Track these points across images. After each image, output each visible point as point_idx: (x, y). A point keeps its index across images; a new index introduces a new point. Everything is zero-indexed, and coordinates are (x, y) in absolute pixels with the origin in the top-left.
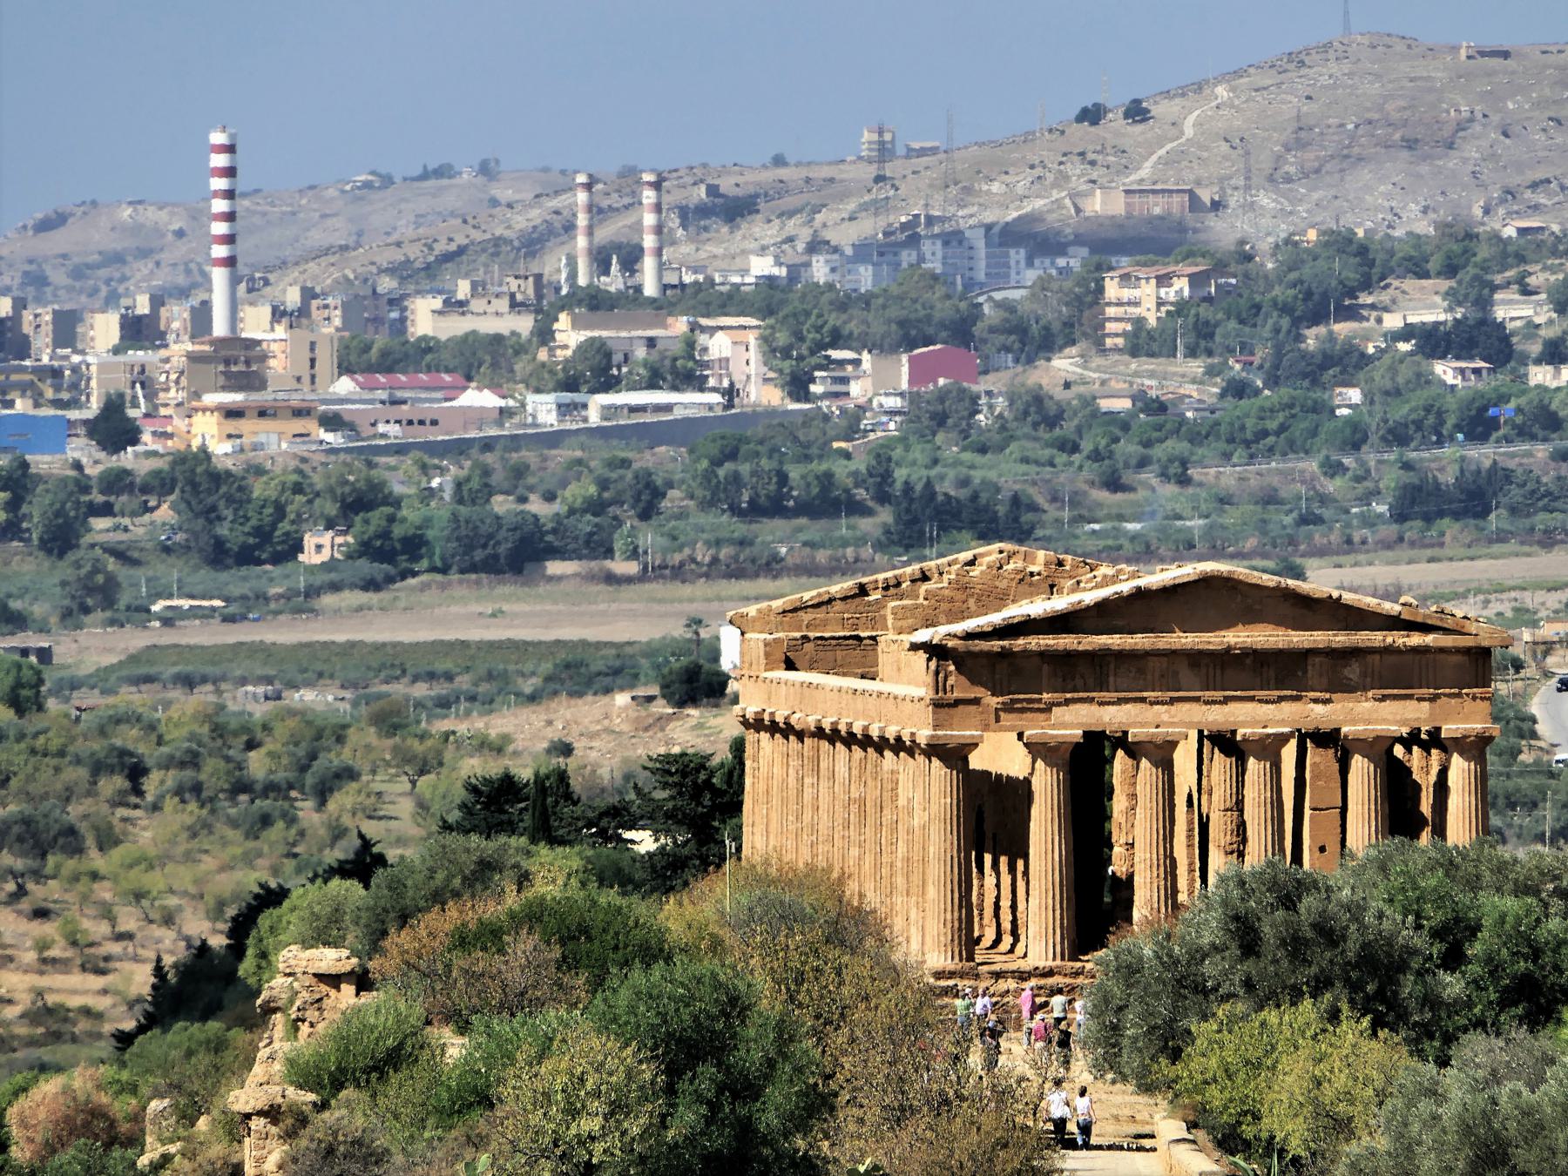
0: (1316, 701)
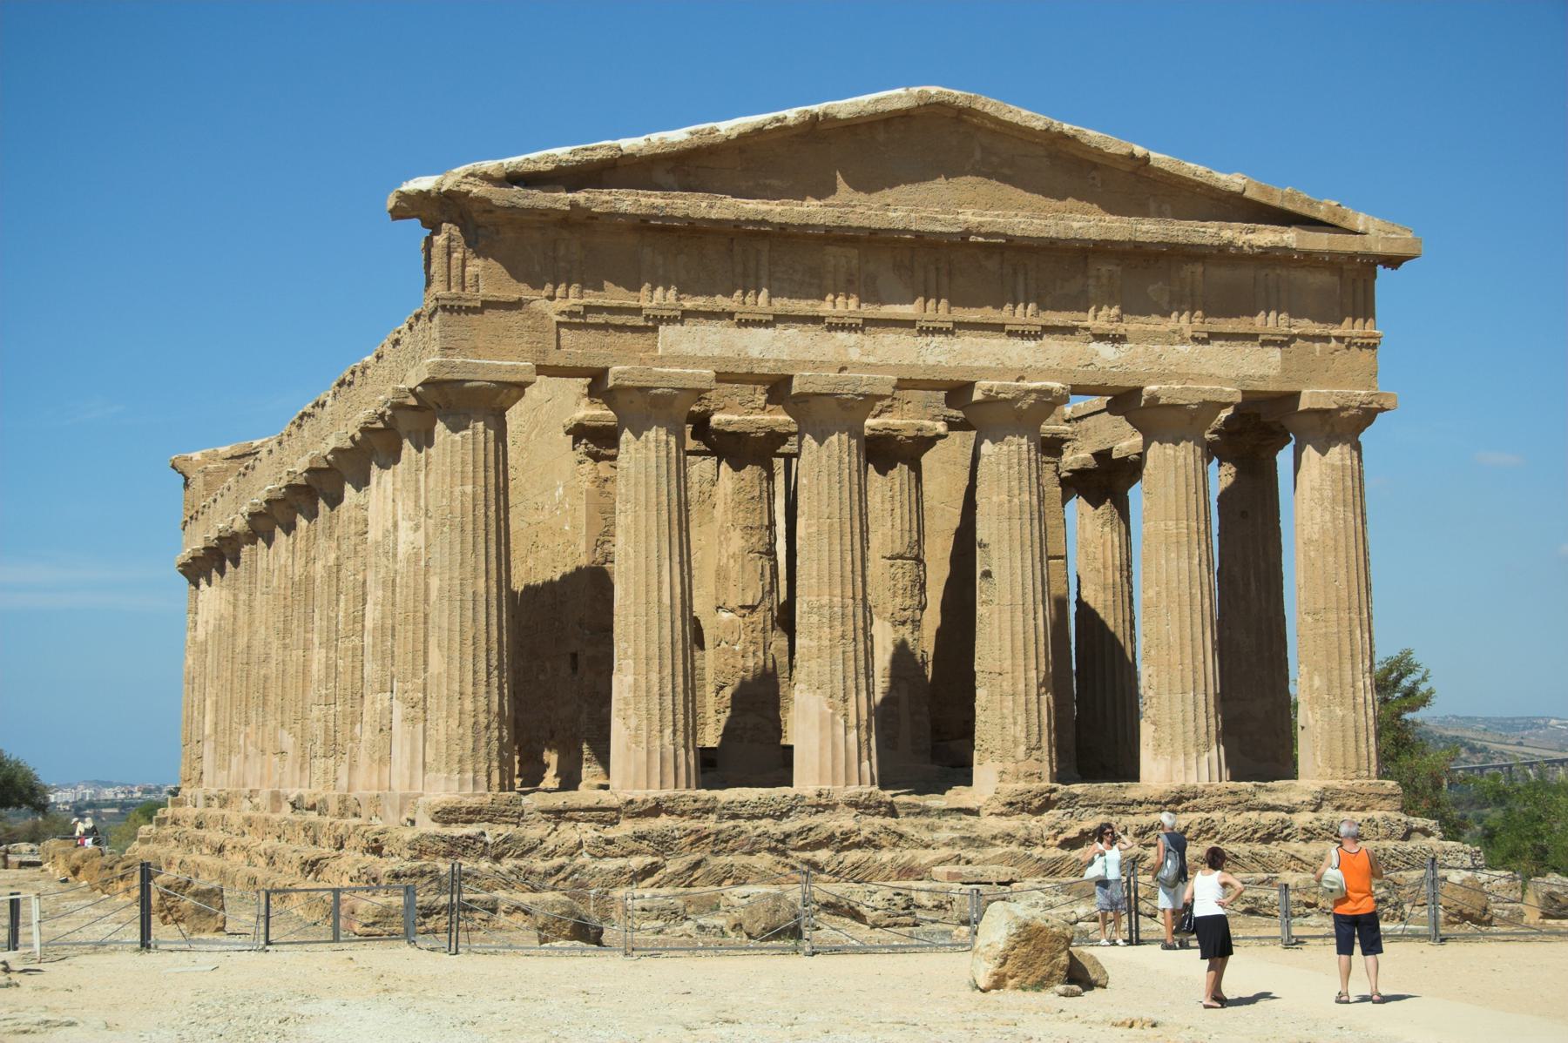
0: (1101, 337)
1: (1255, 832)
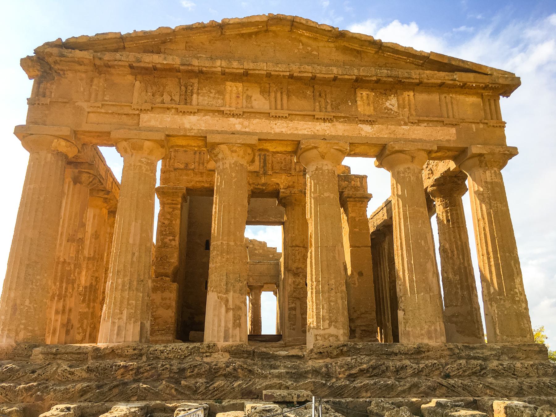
1: (464, 371)
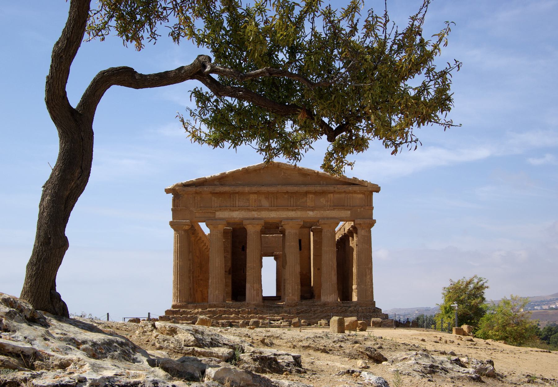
1: (339, 311)
